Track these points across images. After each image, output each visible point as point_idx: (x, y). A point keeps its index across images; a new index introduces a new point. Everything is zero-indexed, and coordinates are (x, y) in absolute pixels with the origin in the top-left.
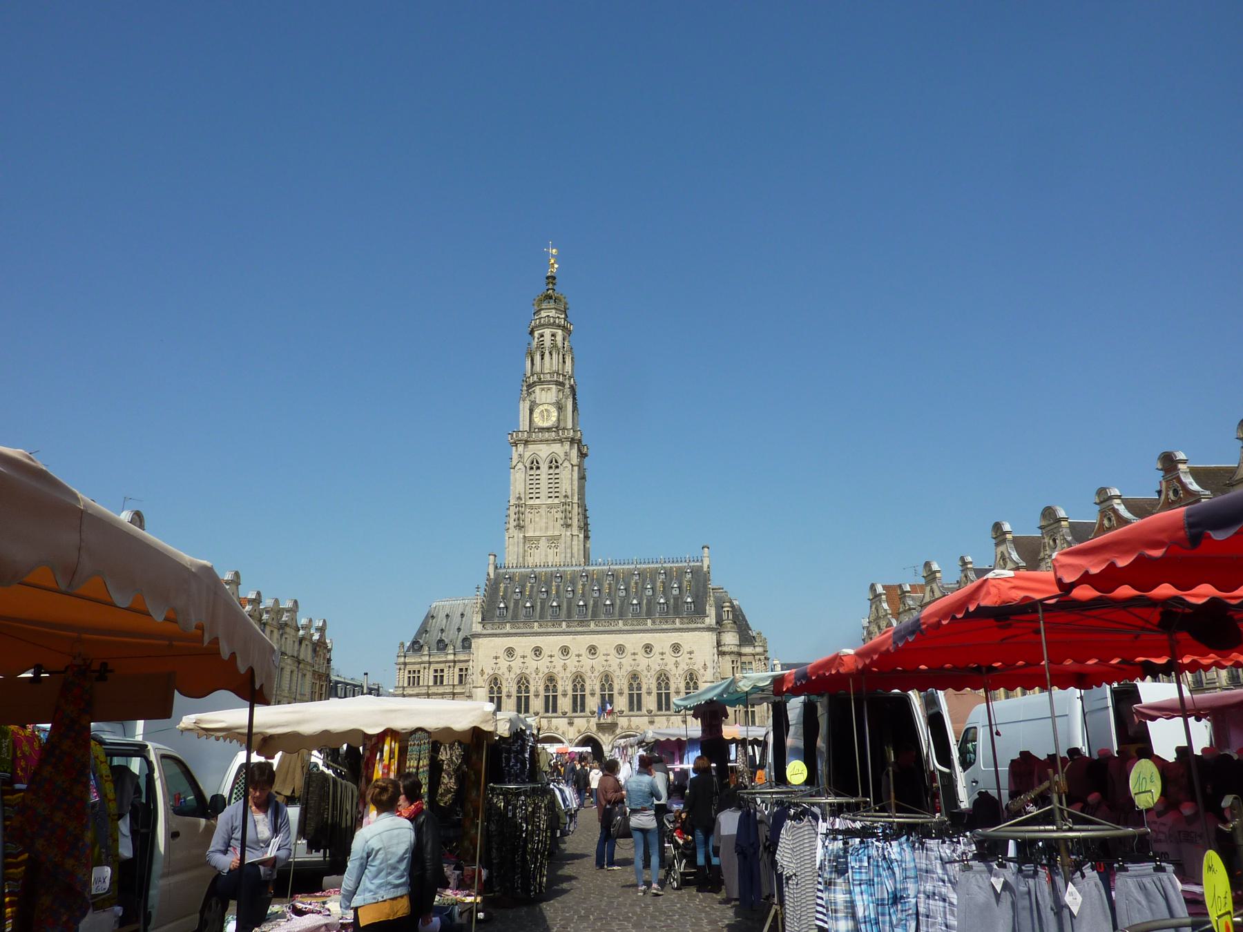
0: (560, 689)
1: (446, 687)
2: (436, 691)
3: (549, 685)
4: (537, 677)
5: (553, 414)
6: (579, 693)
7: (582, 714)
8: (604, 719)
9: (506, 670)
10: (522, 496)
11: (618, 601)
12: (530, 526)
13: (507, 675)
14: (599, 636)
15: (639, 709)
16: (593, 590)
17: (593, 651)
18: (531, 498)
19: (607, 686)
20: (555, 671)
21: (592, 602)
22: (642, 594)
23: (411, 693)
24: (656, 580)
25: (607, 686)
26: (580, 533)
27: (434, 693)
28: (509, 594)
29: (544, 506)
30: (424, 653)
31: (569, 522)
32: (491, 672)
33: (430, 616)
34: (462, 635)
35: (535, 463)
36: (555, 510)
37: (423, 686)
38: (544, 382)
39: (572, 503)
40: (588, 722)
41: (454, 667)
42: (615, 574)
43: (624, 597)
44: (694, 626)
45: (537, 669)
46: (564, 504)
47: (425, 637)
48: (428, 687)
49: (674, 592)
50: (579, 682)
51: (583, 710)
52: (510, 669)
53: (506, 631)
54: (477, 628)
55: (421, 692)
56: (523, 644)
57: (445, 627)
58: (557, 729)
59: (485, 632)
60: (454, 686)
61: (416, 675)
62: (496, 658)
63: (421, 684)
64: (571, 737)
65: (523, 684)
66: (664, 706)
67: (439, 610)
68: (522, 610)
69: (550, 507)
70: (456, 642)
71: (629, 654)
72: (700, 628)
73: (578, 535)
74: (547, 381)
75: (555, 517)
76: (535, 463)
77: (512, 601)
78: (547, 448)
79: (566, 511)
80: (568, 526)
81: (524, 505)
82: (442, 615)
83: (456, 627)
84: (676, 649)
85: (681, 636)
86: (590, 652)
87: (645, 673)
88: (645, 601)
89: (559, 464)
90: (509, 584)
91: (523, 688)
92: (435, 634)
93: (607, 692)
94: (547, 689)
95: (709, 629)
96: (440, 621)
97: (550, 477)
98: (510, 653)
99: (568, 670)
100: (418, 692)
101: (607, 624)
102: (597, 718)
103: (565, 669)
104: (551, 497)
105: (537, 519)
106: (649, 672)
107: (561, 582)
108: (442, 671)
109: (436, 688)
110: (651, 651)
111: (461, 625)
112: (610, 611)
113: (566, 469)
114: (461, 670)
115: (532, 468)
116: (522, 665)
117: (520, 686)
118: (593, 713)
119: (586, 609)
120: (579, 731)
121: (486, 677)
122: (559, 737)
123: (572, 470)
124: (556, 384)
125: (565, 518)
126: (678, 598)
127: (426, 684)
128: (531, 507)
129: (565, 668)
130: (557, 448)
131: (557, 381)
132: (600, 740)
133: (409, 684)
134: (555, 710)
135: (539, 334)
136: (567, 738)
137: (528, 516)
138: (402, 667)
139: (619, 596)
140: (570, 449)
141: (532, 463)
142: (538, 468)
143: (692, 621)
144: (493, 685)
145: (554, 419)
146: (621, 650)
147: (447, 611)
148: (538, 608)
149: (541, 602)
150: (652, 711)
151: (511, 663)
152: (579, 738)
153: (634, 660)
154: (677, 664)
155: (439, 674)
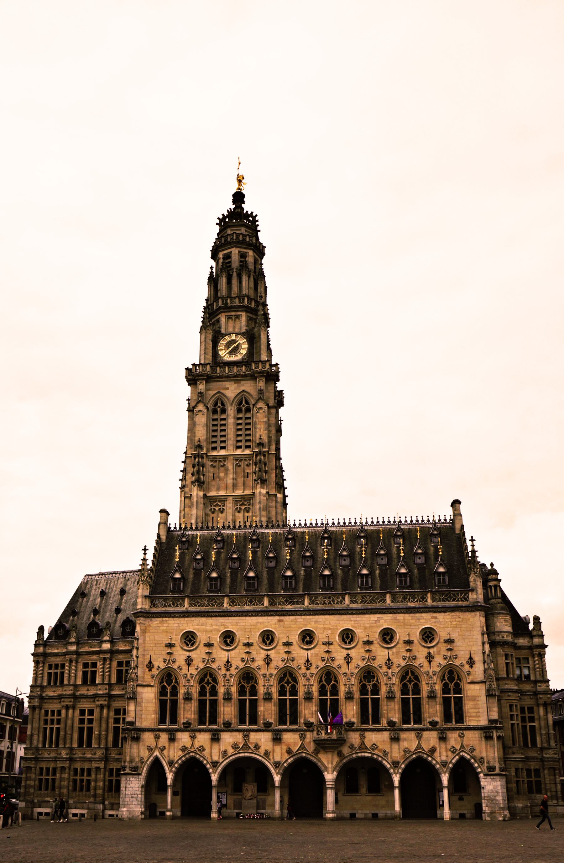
0: (261, 690)
1: (99, 687)
2: (85, 693)
3: (246, 685)
4: (228, 673)
5: (243, 346)
6: (288, 697)
7: (294, 727)
8: (327, 733)
9: (184, 663)
10: (204, 444)
11: (340, 572)
12: (213, 483)
13: (185, 670)
14: (317, 617)
15: (376, 720)
16: (304, 557)
17: (308, 639)
18: (214, 449)
19: (328, 688)
20: (254, 665)
21: (302, 573)
22: (372, 563)
23: (52, 694)
24: (390, 546)
25: (328, 688)
26: (280, 493)
27: (83, 695)
28: (187, 562)
29: (232, 457)
30: (71, 641)
31: (265, 476)
32: (163, 666)
33: (79, 593)
34: (121, 618)
35: (219, 404)
36: (246, 463)
37: (69, 685)
38: (231, 307)
39: (269, 454)
40: (303, 738)
41: (111, 660)
42: (333, 537)
43: (348, 566)
44: (453, 604)
45: (228, 662)
46: (258, 454)
47: (73, 620)
48: (75, 686)
49: (419, 561)
50: (288, 683)
51: (294, 721)
52: (189, 661)
53: (184, 608)
54: (142, 604)
55: (64, 693)
56: (208, 628)
57: (100, 607)
58: (257, 747)
59: (155, 610)
60: (110, 685)
61: (59, 671)
62: (170, 646)
63: (66, 682)
64: (278, 758)
65: (208, 683)
66: (412, 715)
67: (91, 587)
68: (205, 582)
69: (238, 459)
70: (114, 627)
71: (361, 643)
72: (462, 607)
73: (276, 494)
74: (235, 307)
75: (247, 471)
76: (219, 404)
77: (192, 571)
78: (236, 385)
79: (260, 462)
80: (263, 482)
81: (205, 456)
82: (95, 592)
83: (114, 607)
84: (428, 637)
85: (436, 618)
86: (303, 640)
87: (385, 669)
88: (377, 572)
89: (251, 406)
90: (187, 549)
91: (208, 688)
92: (86, 616)
93: (328, 697)
94: (242, 691)
95: (473, 608)
96: (94, 599)
97: (240, 421)
98: (190, 641)
99: (273, 665)
100: (60, 693)
101: (327, 601)
102: (315, 733)
103: (268, 664)
104: (240, 447)
105: (222, 475)
106: (389, 668)
107: (258, 547)
108: (94, 665)
109: (85, 689)
110: (391, 639)
111: (120, 603)
112: (329, 585)
113: (261, 411)
114: (120, 664)
115: (215, 412)
116: (206, 657)
117: (203, 686)
118: (309, 725)
119: (296, 583)
120: (289, 751)
121: (155, 672)
122: (260, 758)
123: (269, 413)
124: (246, 311)
125: (260, 471)
126: (424, 568)
127: (72, 682)
128: (214, 458)
129: (268, 660)
130: (248, 386)
131: (247, 307)
132: (319, 764)
133: (49, 683)
134: (254, 720)
135: (224, 255)
136: (272, 761)
137: (209, 472)
138: (41, 659)
139: (341, 566)
140: (267, 388)
141: (216, 404)
142: (224, 411)
143: (451, 597)
144: (165, 684)
145: (244, 352)
146: (348, 638)
147: (102, 586)
148: (228, 580)
149: (231, 573)
150: (395, 723)
151: (190, 654)
152: (289, 761)
153: (368, 651)
154: (430, 658)
155: (90, 669)
